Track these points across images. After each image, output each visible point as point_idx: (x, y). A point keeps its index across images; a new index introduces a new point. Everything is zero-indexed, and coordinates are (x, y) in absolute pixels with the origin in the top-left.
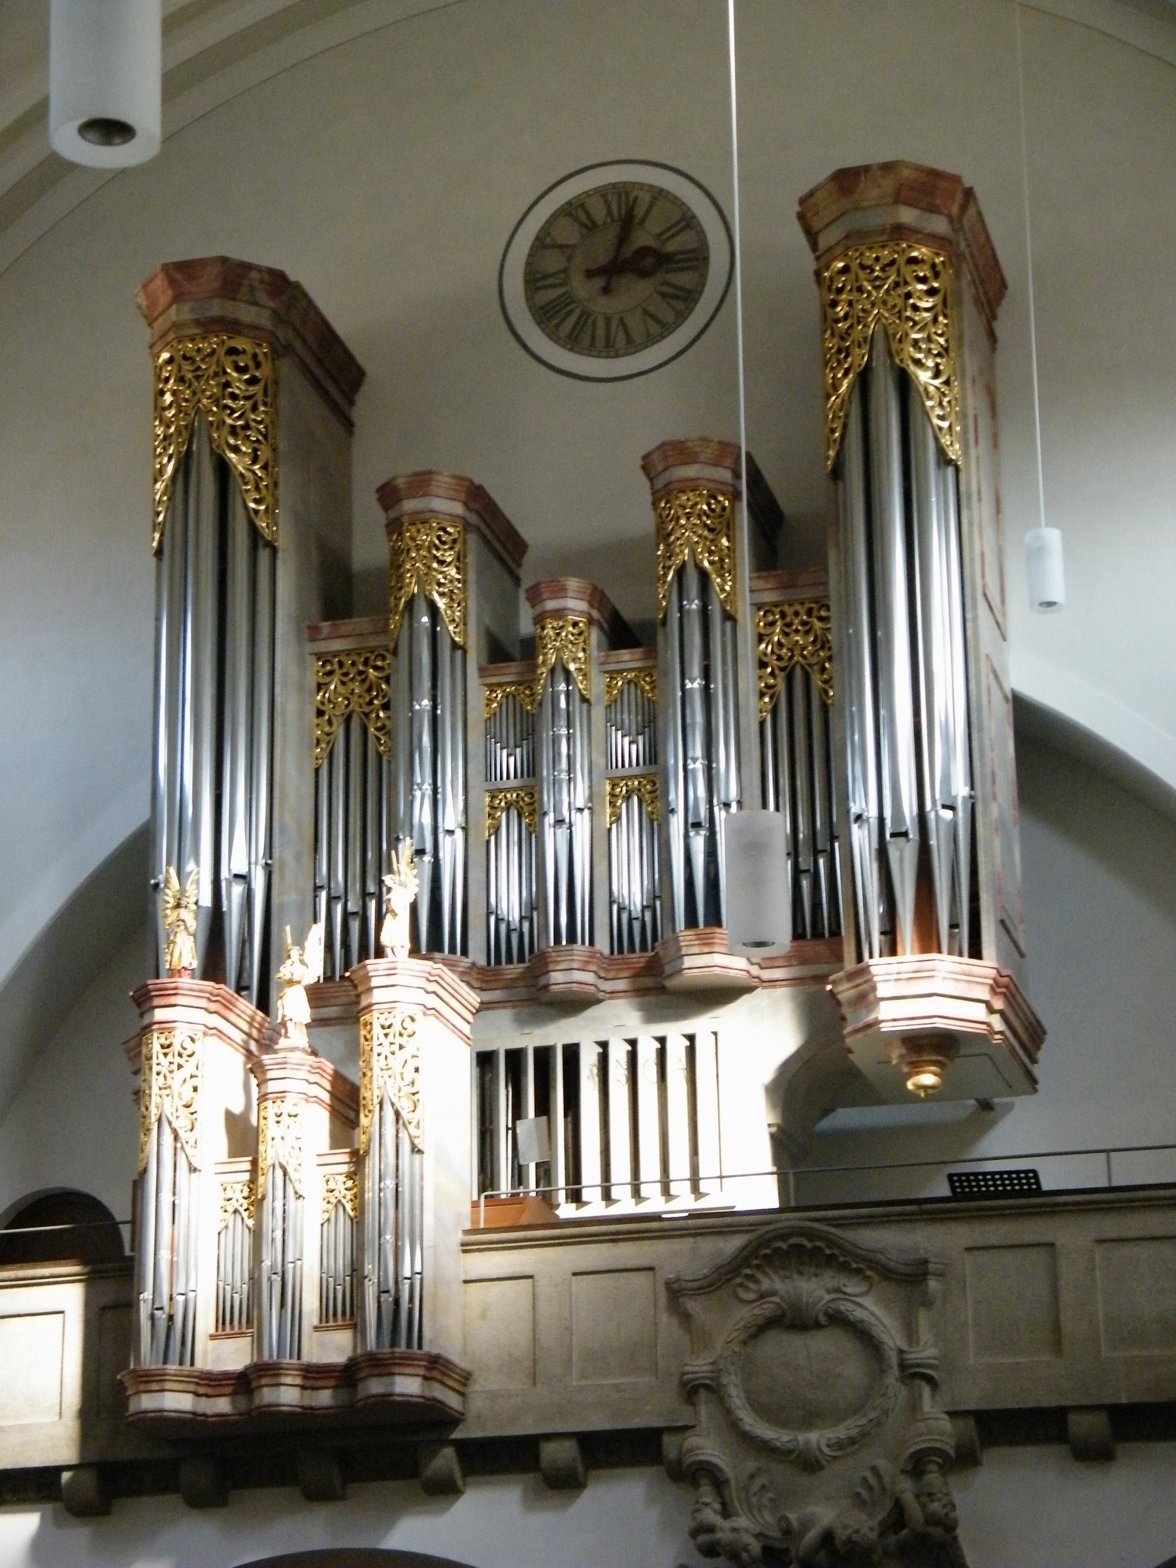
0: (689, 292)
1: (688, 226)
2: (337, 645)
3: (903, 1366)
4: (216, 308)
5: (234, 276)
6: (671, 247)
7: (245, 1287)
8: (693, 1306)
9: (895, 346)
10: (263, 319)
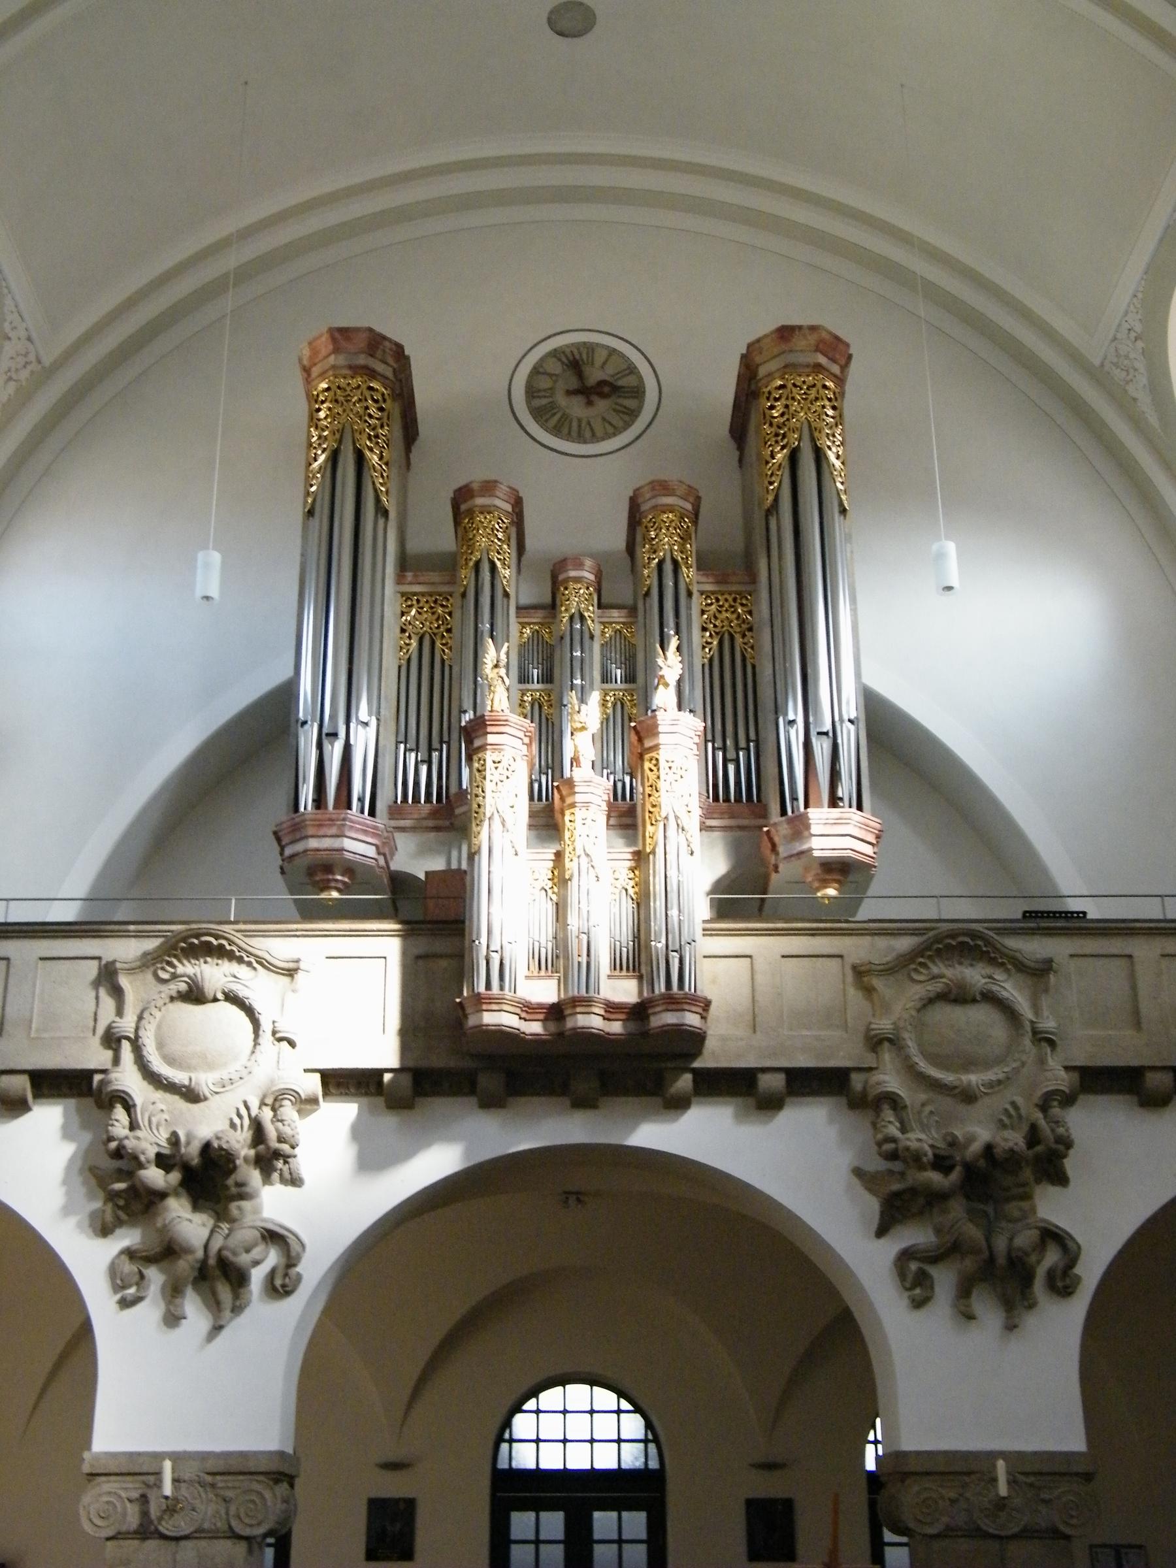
0: (633, 411)
1: (631, 373)
3: (1035, 1032)
4: (362, 360)
5: (375, 342)
6: (620, 383)
7: (550, 944)
8: (876, 982)
9: (816, 434)
10: (389, 373)
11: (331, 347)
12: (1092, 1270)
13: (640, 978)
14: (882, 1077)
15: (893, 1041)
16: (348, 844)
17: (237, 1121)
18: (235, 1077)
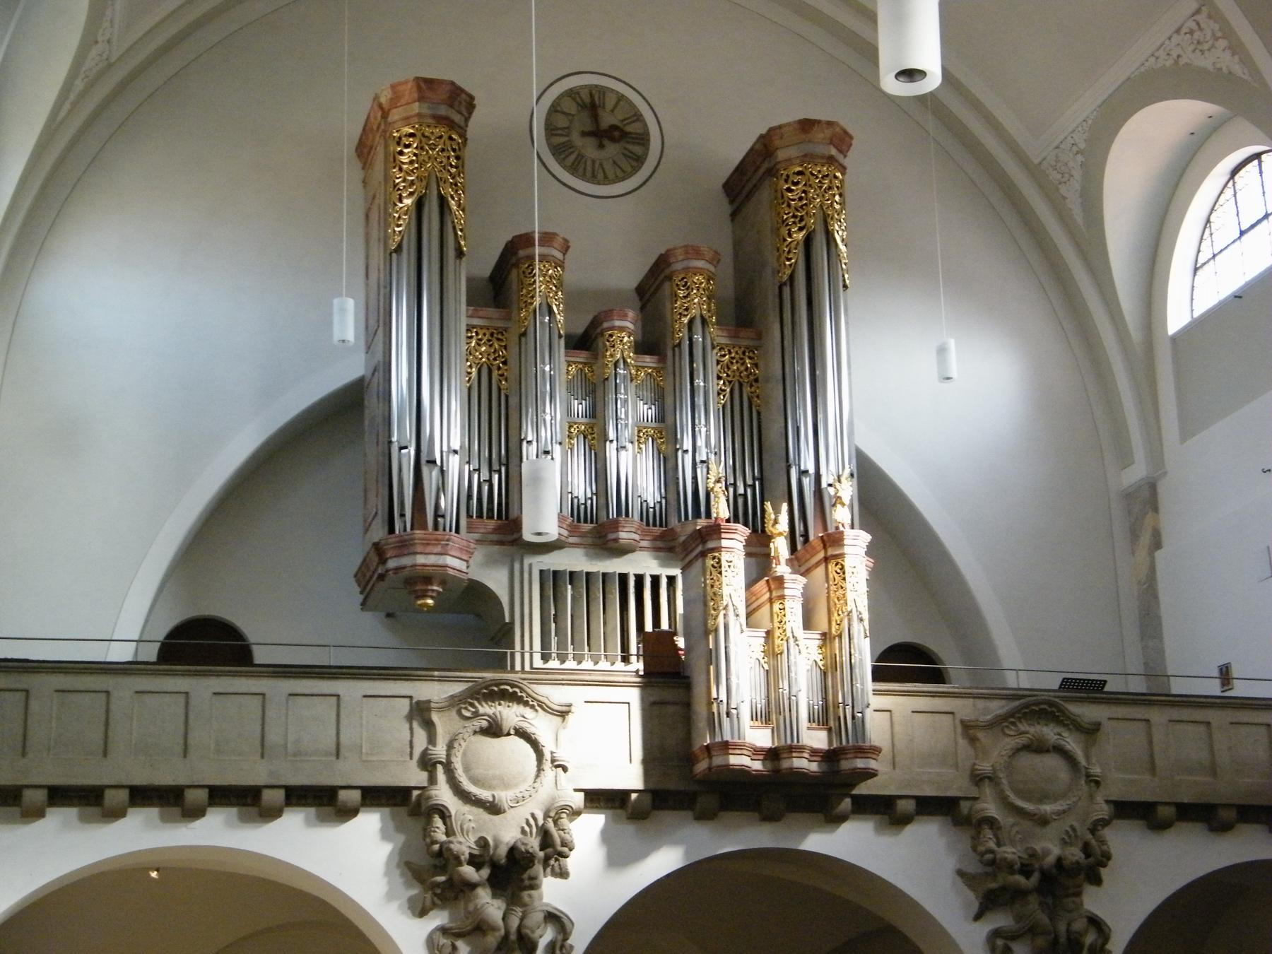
1: (638, 120)
2: (476, 322)
4: (443, 111)
6: (629, 129)
8: (980, 734)
11: (416, 95)
13: (830, 730)
14: (985, 805)
15: (992, 779)
16: (449, 561)
17: (527, 829)
18: (526, 794)
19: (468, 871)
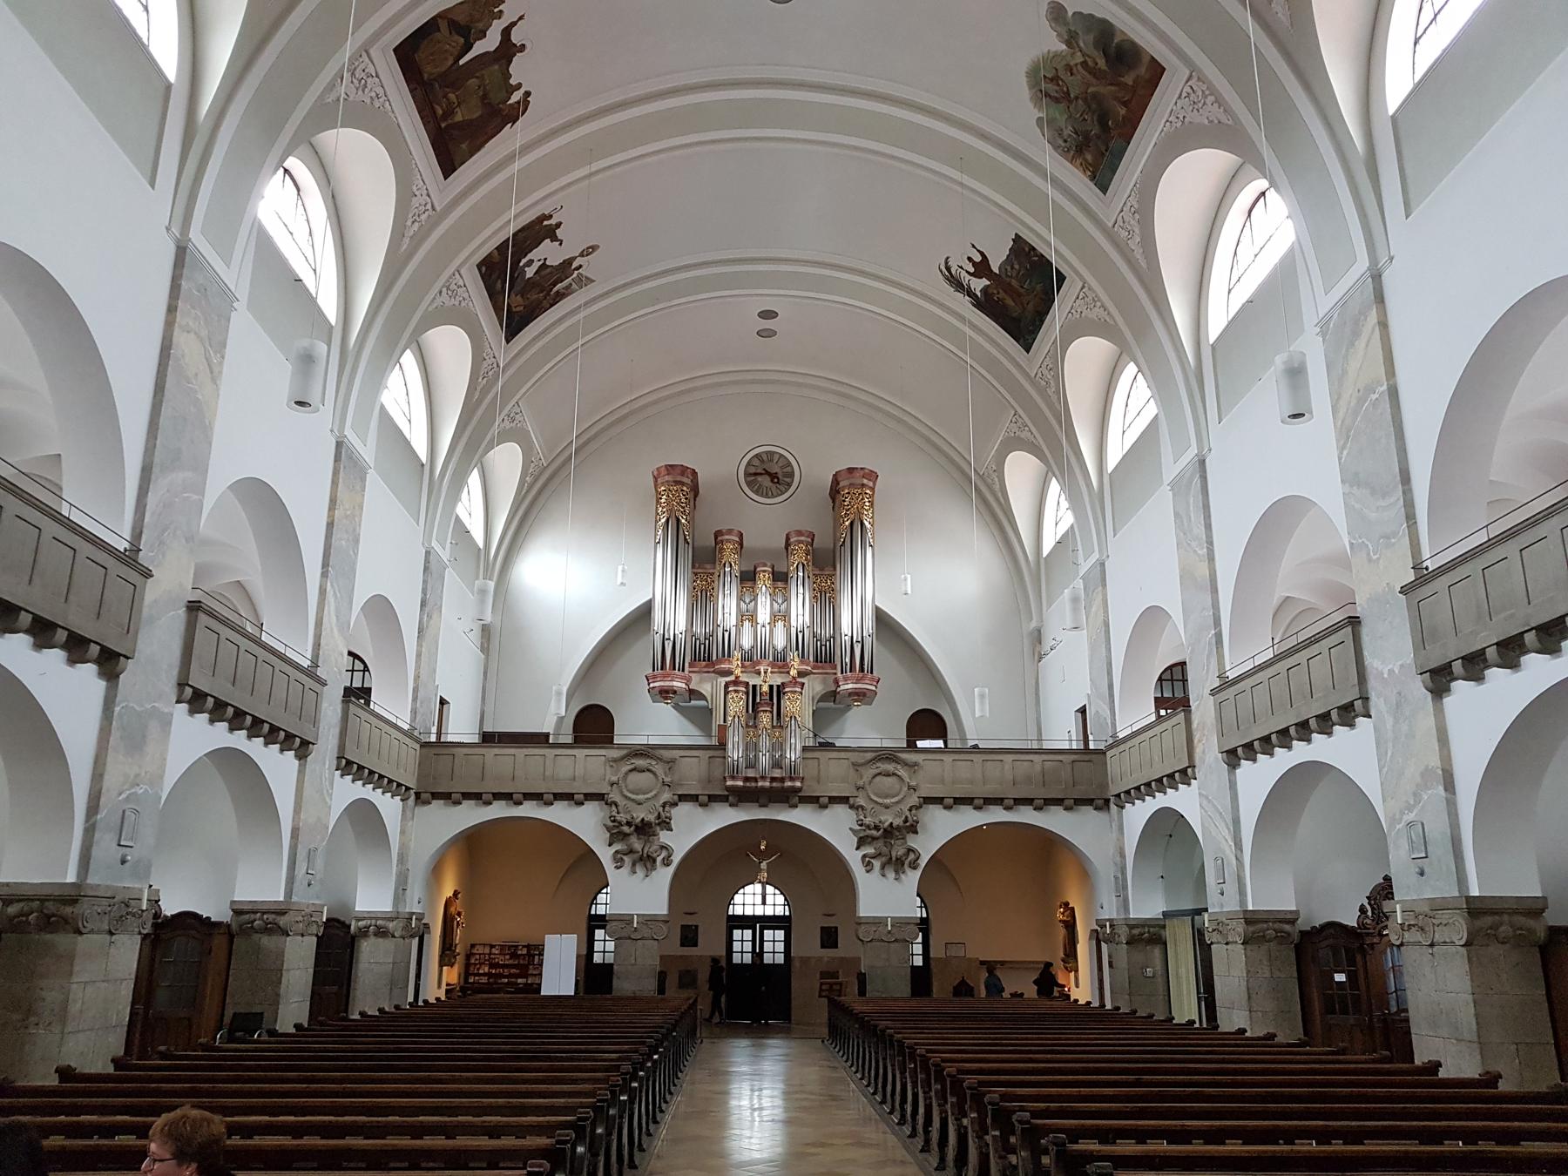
5: (684, 470)
12: (923, 862)
19: (626, 829)
